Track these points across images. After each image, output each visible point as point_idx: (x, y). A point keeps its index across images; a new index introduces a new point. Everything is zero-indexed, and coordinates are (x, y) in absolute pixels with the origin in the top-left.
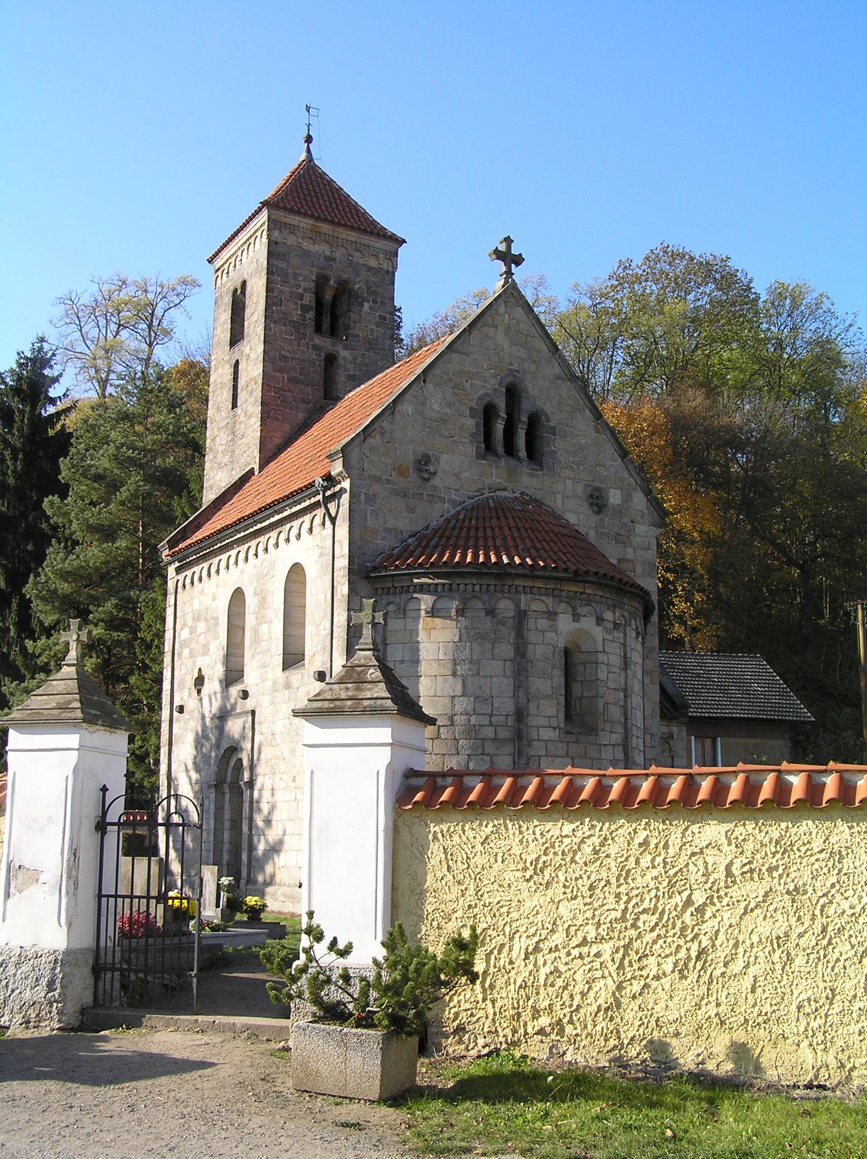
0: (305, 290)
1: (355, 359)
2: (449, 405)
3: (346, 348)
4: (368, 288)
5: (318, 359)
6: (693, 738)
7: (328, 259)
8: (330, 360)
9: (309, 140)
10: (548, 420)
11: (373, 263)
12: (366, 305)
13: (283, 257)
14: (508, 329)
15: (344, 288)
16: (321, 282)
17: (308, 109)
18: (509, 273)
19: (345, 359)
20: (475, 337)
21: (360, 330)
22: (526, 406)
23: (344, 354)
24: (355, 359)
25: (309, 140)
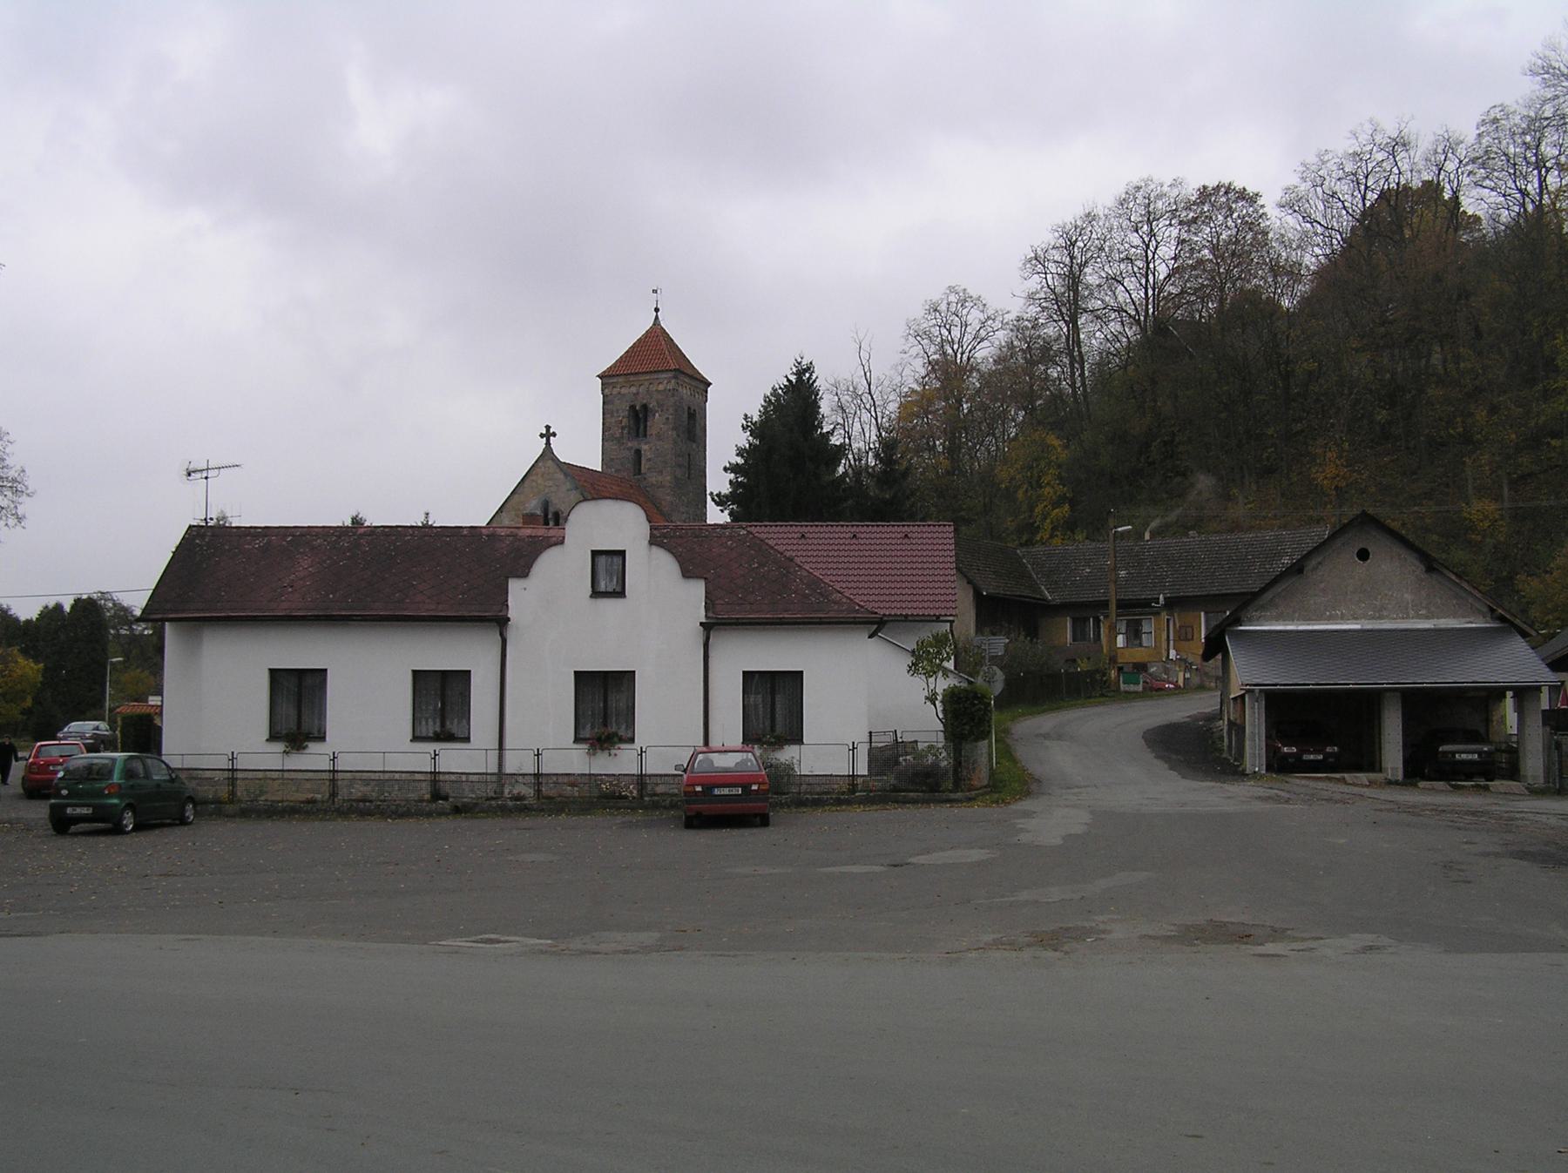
0: (623, 417)
1: (651, 449)
2: (512, 521)
3: (646, 444)
4: (658, 403)
5: (630, 455)
6: (1202, 614)
7: (634, 394)
8: (638, 452)
9: (657, 310)
10: (562, 513)
11: (661, 387)
12: (657, 415)
13: (612, 402)
14: (542, 476)
15: (645, 407)
16: (633, 407)
17: (655, 291)
18: (548, 443)
19: (645, 451)
20: (527, 482)
21: (652, 431)
22: (551, 510)
23: (645, 447)
24: (651, 449)
25: (657, 310)
